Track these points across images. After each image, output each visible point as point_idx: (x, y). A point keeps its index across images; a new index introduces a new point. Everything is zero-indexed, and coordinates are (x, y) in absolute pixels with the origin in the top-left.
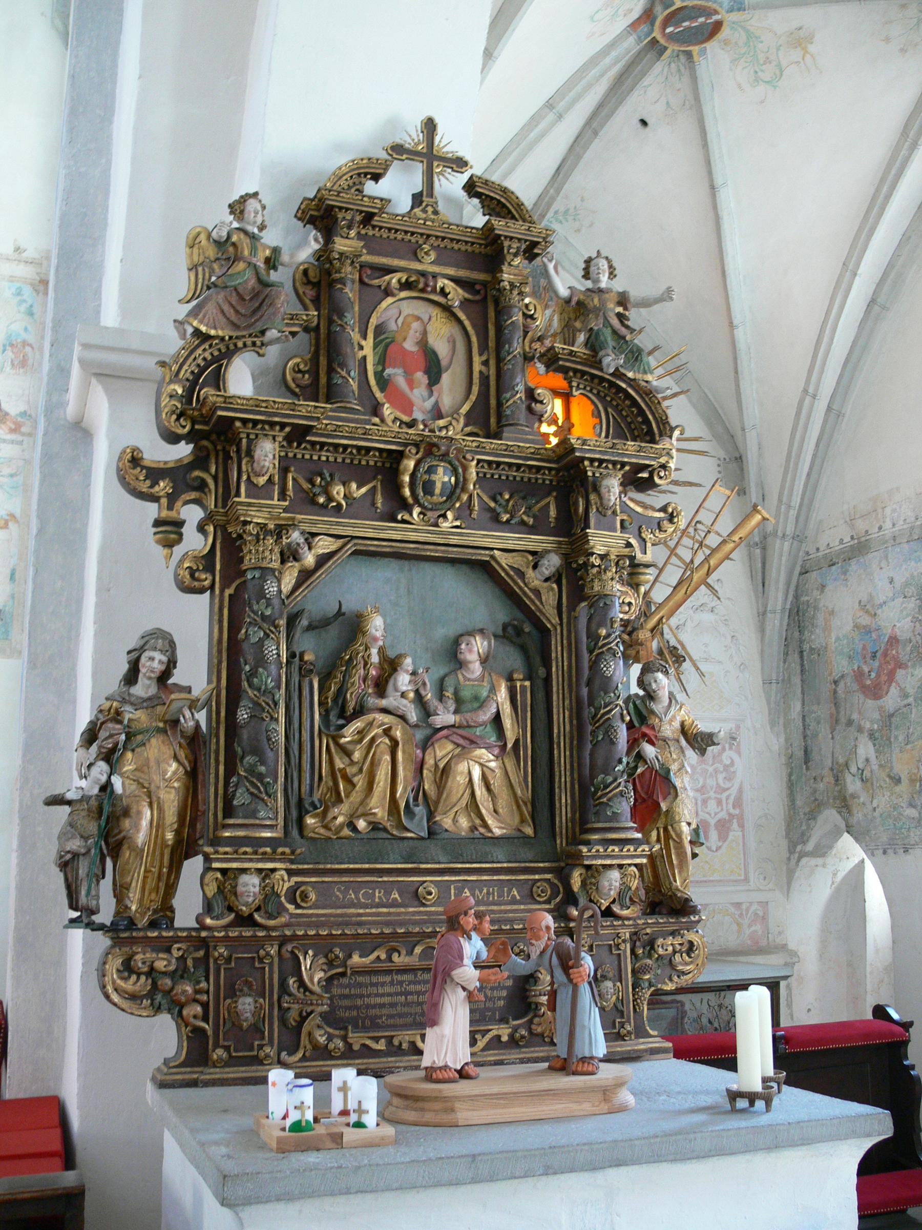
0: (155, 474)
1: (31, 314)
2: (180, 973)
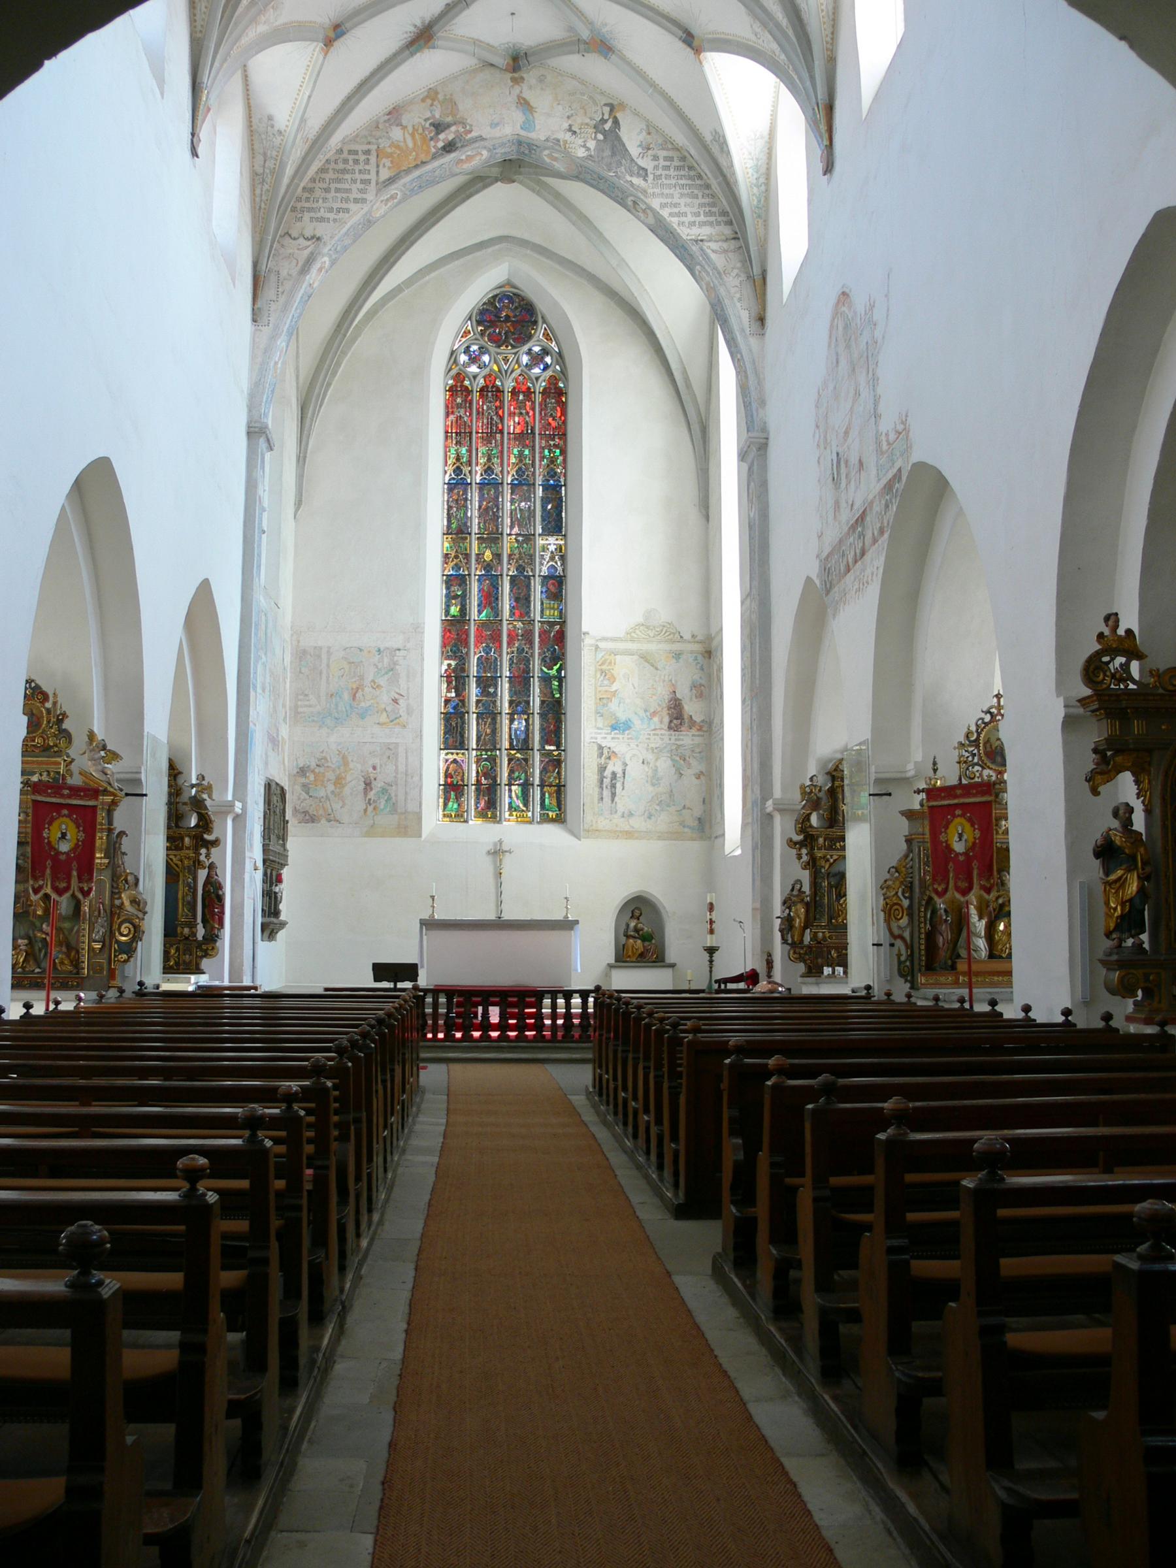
0: (796, 843)
1: (702, 669)
2: (806, 953)
